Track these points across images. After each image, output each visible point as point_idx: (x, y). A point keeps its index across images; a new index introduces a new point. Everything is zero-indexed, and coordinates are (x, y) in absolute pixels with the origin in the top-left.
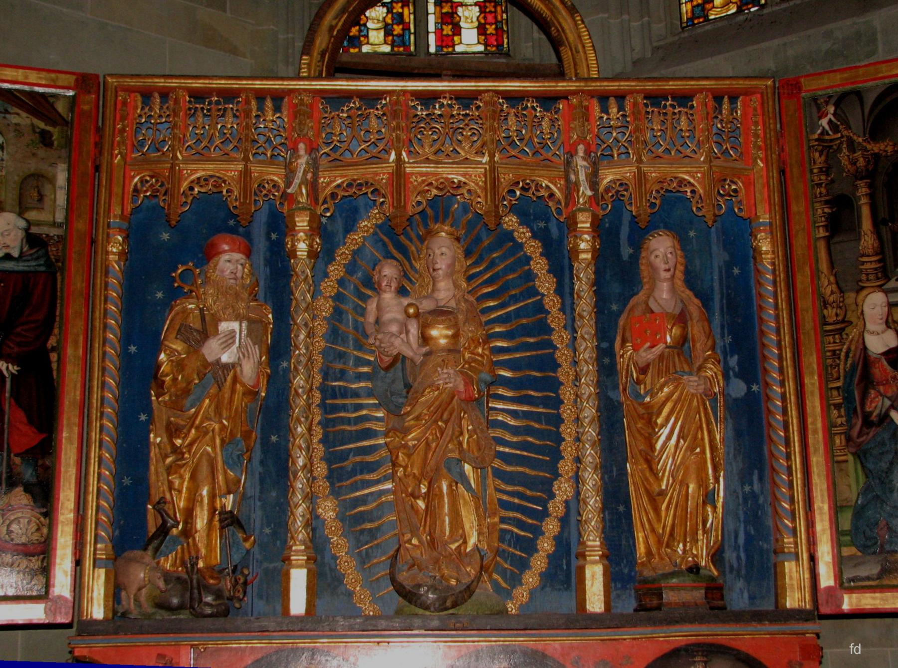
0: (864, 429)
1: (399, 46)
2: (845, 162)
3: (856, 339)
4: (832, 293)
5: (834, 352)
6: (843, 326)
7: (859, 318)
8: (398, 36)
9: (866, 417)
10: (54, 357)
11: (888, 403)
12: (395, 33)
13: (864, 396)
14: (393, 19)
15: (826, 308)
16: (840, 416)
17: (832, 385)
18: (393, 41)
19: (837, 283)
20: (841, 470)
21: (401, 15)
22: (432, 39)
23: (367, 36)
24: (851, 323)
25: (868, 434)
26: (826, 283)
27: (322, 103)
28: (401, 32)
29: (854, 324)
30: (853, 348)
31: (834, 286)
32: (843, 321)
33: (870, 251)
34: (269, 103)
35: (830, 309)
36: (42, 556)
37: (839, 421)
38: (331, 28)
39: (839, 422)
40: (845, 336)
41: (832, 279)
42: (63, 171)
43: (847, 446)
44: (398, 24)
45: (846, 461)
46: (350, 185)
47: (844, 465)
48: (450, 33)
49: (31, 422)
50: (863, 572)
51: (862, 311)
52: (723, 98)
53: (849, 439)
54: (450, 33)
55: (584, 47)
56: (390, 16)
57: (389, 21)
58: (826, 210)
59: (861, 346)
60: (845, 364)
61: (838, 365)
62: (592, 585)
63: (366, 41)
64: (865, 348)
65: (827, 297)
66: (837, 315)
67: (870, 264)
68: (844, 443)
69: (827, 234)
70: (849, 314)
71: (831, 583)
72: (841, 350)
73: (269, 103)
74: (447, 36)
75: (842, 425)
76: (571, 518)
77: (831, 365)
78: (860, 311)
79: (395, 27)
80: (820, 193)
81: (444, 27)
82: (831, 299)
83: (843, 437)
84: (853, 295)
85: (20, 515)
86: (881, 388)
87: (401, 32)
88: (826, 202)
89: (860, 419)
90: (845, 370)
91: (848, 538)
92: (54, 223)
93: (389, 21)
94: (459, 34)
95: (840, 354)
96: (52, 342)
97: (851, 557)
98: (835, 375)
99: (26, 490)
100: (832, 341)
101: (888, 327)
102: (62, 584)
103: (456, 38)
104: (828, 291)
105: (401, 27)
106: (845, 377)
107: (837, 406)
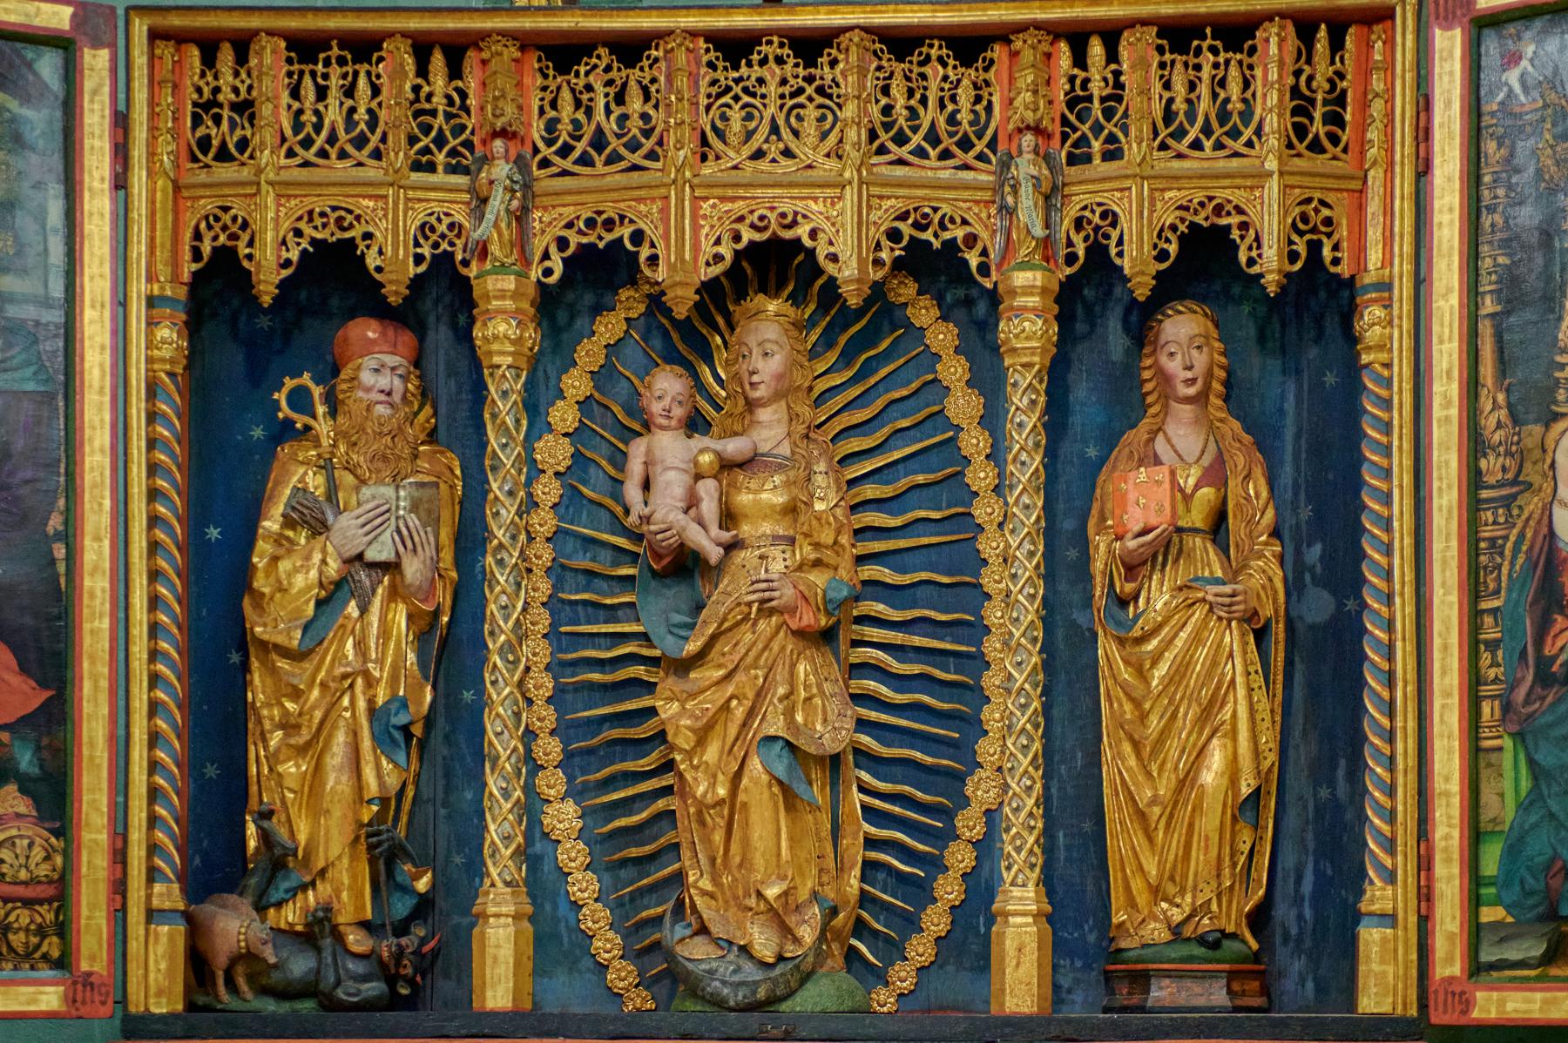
3: (1536, 516)
4: (1499, 425)
5: (1492, 540)
6: (1514, 490)
7: (1545, 475)
10: (60, 551)
15: (1485, 455)
16: (1494, 664)
17: (1484, 605)
19: (1510, 406)
20: (1489, 765)
25: (1543, 699)
26: (1489, 407)
27: (539, 60)
29: (1536, 486)
30: (1529, 534)
31: (1503, 413)
34: (438, 61)
35: (1492, 458)
36: (56, 904)
37: (1492, 673)
39: (1492, 676)
40: (1515, 512)
41: (1501, 397)
42: (56, 197)
43: (1503, 720)
45: (1500, 749)
46: (590, 223)
47: (1494, 757)
49: (24, 669)
50: (1513, 953)
51: (1553, 462)
52: (1317, 29)
53: (1507, 708)
58: (1501, 260)
59: (1545, 530)
60: (1512, 564)
61: (1499, 567)
62: (1018, 965)
64: (1552, 534)
65: (1487, 433)
66: (1504, 469)
68: (1497, 714)
69: (1499, 308)
70: (1528, 467)
72: (1506, 538)
73: (438, 61)
75: (1496, 680)
76: (986, 847)
77: (1485, 568)
78: (1549, 461)
80: (1493, 225)
82: (1497, 438)
83: (1497, 703)
84: (1537, 429)
85: (14, 832)
89: (1531, 671)
90: (1510, 575)
92: (47, 298)
95: (1503, 546)
96: (55, 523)
97: (1497, 925)
98: (1492, 586)
99: (23, 790)
100: (1491, 520)
102: (92, 953)
104: (1492, 422)
106: (1510, 590)
107: (1492, 646)
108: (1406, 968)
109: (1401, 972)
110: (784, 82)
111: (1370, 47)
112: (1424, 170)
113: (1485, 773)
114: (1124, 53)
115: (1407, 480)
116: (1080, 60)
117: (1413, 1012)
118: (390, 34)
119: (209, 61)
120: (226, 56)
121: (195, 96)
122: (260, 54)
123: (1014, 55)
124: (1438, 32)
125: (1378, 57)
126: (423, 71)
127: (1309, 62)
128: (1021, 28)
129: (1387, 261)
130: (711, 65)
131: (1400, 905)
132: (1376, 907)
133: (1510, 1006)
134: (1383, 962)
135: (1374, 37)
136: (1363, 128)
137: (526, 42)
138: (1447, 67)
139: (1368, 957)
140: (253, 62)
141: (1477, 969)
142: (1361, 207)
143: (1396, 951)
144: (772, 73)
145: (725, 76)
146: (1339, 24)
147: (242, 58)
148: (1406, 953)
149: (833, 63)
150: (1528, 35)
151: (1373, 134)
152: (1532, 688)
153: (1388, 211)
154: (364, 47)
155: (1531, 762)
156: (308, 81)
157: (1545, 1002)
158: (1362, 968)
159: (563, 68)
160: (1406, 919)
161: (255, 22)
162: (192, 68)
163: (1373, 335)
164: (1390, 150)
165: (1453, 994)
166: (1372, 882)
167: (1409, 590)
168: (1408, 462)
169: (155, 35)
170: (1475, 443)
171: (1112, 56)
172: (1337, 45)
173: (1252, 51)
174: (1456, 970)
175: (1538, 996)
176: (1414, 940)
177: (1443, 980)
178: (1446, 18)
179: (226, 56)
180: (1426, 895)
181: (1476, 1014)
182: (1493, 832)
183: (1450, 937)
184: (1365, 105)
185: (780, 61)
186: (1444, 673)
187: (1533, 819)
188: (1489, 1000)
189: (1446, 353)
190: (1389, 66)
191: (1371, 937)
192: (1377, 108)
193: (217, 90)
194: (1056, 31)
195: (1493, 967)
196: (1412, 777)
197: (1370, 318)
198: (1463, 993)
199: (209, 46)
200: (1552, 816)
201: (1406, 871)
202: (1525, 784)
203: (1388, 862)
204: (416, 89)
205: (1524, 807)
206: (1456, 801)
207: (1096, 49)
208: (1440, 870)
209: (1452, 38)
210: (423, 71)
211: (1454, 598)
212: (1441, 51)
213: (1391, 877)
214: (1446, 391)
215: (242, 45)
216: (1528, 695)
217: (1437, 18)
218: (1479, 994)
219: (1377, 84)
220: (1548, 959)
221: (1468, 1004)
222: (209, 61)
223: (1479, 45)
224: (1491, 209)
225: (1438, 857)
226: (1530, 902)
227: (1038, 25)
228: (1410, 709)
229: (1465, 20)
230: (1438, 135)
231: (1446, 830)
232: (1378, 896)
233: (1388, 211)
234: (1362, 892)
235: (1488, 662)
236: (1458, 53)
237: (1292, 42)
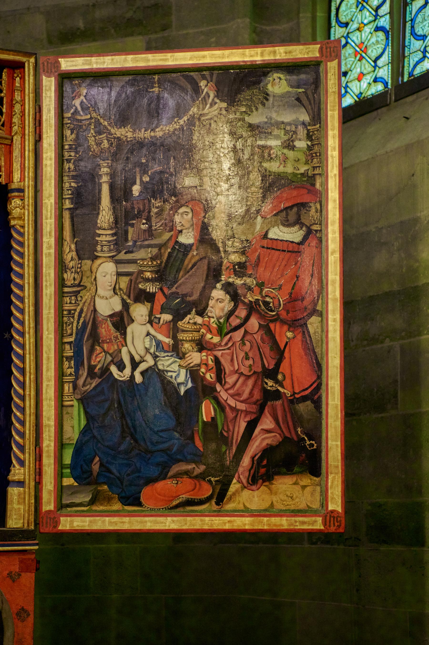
0: (89, 379)
2: (92, 141)
3: (88, 301)
4: (72, 259)
5: (69, 311)
6: (79, 289)
7: (92, 283)
9: (91, 368)
11: (109, 358)
13: (91, 351)
15: (66, 272)
16: (70, 367)
17: (66, 340)
19: (77, 251)
20: (68, 413)
24: (85, 287)
26: (68, 250)
29: (88, 288)
30: (85, 310)
31: (74, 253)
32: (79, 285)
33: (106, 225)
35: (69, 273)
37: (69, 371)
39: (69, 373)
40: (79, 299)
41: (73, 246)
45: (72, 406)
47: (69, 409)
51: (96, 278)
53: (75, 387)
58: (73, 184)
59: (92, 308)
60: (78, 323)
61: (73, 322)
64: (95, 310)
65: (67, 262)
66: (74, 279)
67: (105, 236)
69: (72, 206)
70: (85, 279)
71: (51, 507)
72: (75, 310)
75: (71, 374)
77: (66, 323)
78: (94, 277)
80: (69, 168)
82: (71, 264)
83: (71, 385)
84: (89, 262)
86: (105, 346)
88: (73, 177)
90: (77, 327)
91: (69, 471)
95: (74, 314)
97: (70, 487)
98: (69, 332)
100: (68, 302)
101: (116, 293)
104: (69, 257)
106: (77, 334)
107: (69, 359)
108: (29, 507)
109: (27, 508)
111: (14, 80)
112: (38, 140)
113: (65, 417)
115: (32, 280)
117: (32, 527)
124: (44, 77)
125: (17, 85)
129: (22, 179)
131: (27, 477)
132: (16, 478)
133: (75, 524)
134: (19, 503)
135: (15, 75)
136: (11, 116)
138: (48, 93)
139: (12, 501)
141: (61, 506)
142: (10, 152)
143: (24, 498)
148: (29, 500)
150: (84, 85)
151: (15, 120)
152: (86, 378)
153: (23, 156)
155: (86, 413)
157: (91, 522)
158: (9, 507)
160: (29, 484)
163: (16, 212)
164: (23, 128)
165: (50, 518)
166: (14, 466)
167: (32, 331)
168: (32, 272)
170: (61, 266)
174: (51, 507)
175: (88, 519)
176: (33, 493)
177: (46, 512)
178: (47, 72)
180: (39, 473)
181: (60, 528)
182: (68, 444)
183: (49, 492)
184: (11, 106)
186: (48, 370)
187: (86, 438)
188: (66, 521)
189: (49, 224)
190: (23, 90)
191: (13, 492)
192: (17, 108)
195: (68, 506)
196: (33, 417)
197: (15, 205)
198: (55, 518)
200: (94, 437)
201: (30, 461)
202: (83, 423)
203: (22, 457)
205: (83, 433)
206: (53, 429)
208: (45, 461)
209: (50, 81)
211: (52, 336)
212: (46, 86)
213: (22, 463)
214: (49, 241)
216: (85, 381)
217: (44, 71)
218: (61, 518)
219: (17, 96)
220: (92, 502)
221: (57, 523)
223: (62, 86)
224: (69, 161)
225: (44, 455)
226: (85, 476)
228: (32, 386)
229: (56, 74)
230: (44, 125)
231: (48, 442)
232: (17, 473)
233: (23, 156)
234: (9, 471)
235: (67, 366)
236: (53, 88)
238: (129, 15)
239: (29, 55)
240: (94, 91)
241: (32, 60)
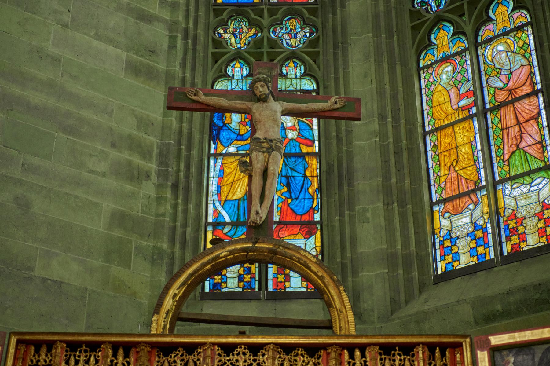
1: (247, 289)
8: (247, 282)
12: (245, 280)
14: (244, 270)
18: (244, 286)
21: (250, 269)
22: (270, 283)
23: (226, 282)
27: (158, 352)
28: (249, 280)
34: (121, 352)
38: (175, 295)
44: (247, 274)
48: (283, 280)
52: (436, 349)
54: (283, 280)
55: (345, 308)
56: (242, 269)
57: (242, 273)
63: (225, 286)
73: (121, 352)
74: (281, 282)
79: (245, 276)
81: (279, 276)
87: (249, 280)
93: (242, 273)
94: (289, 281)
103: (286, 283)
105: (249, 276)
110: (245, 361)
111: (455, 356)
114: (368, 355)
116: (352, 356)
118: (104, 342)
119: (37, 351)
120: (44, 350)
121: (30, 363)
122: (56, 349)
123: (328, 354)
124: (479, 352)
125: (458, 359)
126: (115, 355)
127: (434, 360)
128: (331, 345)
130: (219, 355)
135: (456, 352)
137: (153, 345)
138: (483, 364)
140: (53, 351)
144: (241, 358)
145: (224, 359)
146: (444, 347)
147: (49, 350)
149: (263, 355)
150: (511, 355)
154: (94, 346)
156: (72, 358)
159: (166, 355)
161: (56, 338)
162: (31, 353)
169: (19, 342)
171: (363, 355)
172: (443, 355)
173: (413, 355)
178: (481, 348)
179: (44, 350)
185: (244, 354)
193: (39, 361)
194: (343, 346)
199: (38, 345)
204: (112, 361)
207: (358, 353)
209: (484, 354)
210: (115, 355)
212: (481, 358)
215: (50, 345)
217: (478, 347)
222: (37, 351)
223: (494, 357)
227: (336, 344)
229: (488, 348)
236: (487, 359)
237: (427, 353)
238: (537, 296)
239: (465, 336)
240: (520, 358)
241: (468, 340)
